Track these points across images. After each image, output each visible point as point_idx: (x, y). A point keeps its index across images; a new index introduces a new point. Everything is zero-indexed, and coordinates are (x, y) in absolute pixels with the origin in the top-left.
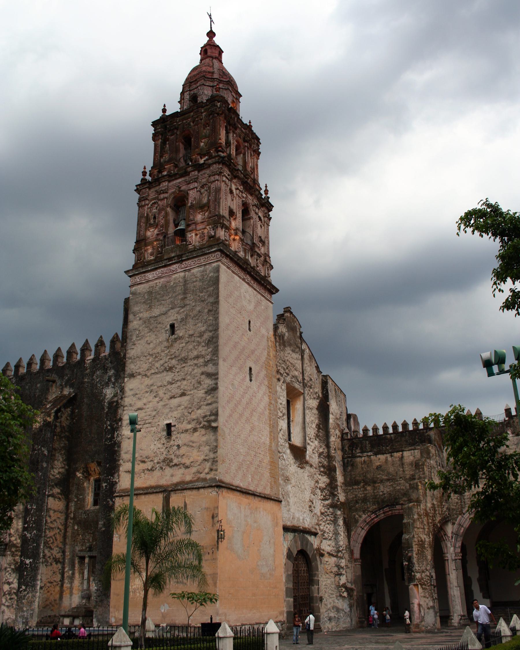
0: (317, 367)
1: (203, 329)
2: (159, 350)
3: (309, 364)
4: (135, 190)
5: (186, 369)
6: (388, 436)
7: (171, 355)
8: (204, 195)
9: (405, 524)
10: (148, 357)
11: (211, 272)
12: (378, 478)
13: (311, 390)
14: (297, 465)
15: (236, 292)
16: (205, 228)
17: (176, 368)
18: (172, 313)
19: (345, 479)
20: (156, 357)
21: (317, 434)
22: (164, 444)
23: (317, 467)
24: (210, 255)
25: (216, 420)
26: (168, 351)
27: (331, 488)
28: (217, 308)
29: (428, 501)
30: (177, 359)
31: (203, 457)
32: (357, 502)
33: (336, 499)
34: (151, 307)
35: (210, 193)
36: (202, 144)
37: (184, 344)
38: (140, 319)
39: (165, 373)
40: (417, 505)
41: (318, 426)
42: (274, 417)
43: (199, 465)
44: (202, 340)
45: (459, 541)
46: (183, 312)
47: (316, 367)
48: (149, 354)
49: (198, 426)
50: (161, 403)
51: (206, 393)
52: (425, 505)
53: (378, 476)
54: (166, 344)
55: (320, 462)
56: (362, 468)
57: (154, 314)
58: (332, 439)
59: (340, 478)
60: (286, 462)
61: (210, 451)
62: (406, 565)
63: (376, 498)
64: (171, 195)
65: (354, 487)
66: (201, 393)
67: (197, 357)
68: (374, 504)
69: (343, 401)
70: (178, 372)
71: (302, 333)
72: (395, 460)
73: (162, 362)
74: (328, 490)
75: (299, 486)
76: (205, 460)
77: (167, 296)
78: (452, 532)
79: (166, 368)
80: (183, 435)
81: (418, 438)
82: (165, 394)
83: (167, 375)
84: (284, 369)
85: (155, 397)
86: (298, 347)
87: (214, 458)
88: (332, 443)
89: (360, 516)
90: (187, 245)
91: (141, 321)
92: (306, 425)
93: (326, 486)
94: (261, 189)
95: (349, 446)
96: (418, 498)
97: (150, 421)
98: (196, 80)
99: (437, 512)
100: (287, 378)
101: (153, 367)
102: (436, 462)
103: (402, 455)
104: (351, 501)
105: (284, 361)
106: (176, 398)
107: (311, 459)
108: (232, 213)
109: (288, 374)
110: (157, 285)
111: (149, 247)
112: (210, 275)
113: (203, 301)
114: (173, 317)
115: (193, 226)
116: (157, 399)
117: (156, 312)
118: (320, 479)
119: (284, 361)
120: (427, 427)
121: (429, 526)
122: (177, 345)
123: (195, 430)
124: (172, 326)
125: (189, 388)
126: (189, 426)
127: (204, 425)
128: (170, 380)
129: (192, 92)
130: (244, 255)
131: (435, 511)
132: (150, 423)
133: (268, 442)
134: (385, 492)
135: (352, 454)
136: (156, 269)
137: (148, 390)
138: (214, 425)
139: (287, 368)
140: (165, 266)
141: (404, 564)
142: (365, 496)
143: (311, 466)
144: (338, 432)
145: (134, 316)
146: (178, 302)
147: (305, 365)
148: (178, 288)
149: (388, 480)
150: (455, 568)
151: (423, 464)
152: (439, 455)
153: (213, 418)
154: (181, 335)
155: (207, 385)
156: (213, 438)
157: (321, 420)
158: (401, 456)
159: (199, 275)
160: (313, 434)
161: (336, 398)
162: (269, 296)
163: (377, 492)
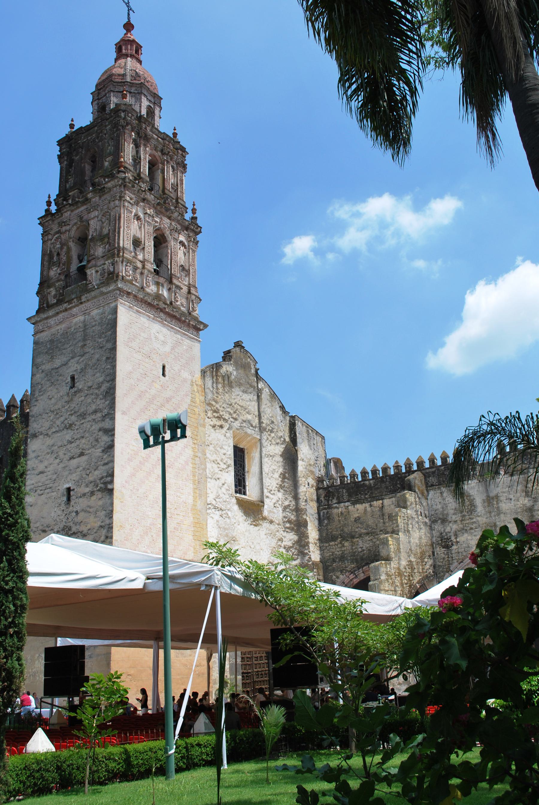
0: (282, 408)
1: (101, 379)
2: (59, 405)
3: (269, 404)
4: (39, 224)
5: (85, 425)
6: (367, 482)
7: (71, 411)
8: (105, 224)
9: (371, 586)
10: (49, 414)
11: (109, 314)
12: (357, 532)
13: (273, 435)
14: (249, 522)
15: (142, 334)
16: (105, 264)
17: (75, 425)
18: (72, 363)
19: (321, 535)
20: (57, 414)
21: (281, 485)
22: (63, 511)
23: (281, 523)
24: (109, 295)
25: (112, 482)
26: (68, 406)
27: (301, 546)
28: (115, 355)
29: (402, 558)
30: (76, 415)
31: (99, 523)
32: (334, 561)
33: (307, 558)
34: (52, 358)
35: (110, 221)
36: (106, 164)
37: (83, 398)
38: (43, 372)
39: (65, 432)
40: (386, 564)
41: (283, 476)
42: (201, 472)
43: (95, 533)
44: (99, 392)
46: (83, 361)
47: (280, 407)
48: (51, 411)
49: (95, 489)
50: (62, 465)
51: (103, 451)
52: (399, 563)
53: (357, 530)
54: (66, 398)
55: (284, 517)
56: (339, 521)
57: (55, 366)
58: (302, 489)
59: (313, 533)
60: (232, 520)
61: (106, 516)
63: (354, 556)
64: (73, 226)
65: (331, 544)
66: (98, 452)
67: (95, 412)
68: (352, 562)
69: (319, 444)
70: (77, 429)
71: (258, 369)
72: (374, 510)
73: (62, 419)
74: (296, 549)
75: (252, 546)
76: (101, 527)
77: (68, 344)
79: (66, 426)
80: (81, 500)
81: (400, 484)
82: (65, 454)
83: (68, 433)
84: (230, 414)
85: (56, 458)
86: (251, 386)
87: (110, 524)
88: (302, 494)
89: (338, 577)
90: (87, 284)
91: (44, 374)
92: (264, 475)
93: (293, 544)
94: (187, 208)
95: (326, 496)
96: (388, 555)
97: (51, 485)
98: (104, 86)
99: (416, 571)
100: (235, 424)
101: (54, 425)
102: (416, 511)
103: (382, 504)
104: (328, 560)
105: (231, 405)
106: (75, 458)
107: (271, 514)
108: (137, 243)
109: (236, 419)
110: (58, 333)
111: (52, 289)
112: (109, 317)
113: (101, 348)
114: (74, 367)
115: (93, 262)
116: (58, 461)
117: (58, 362)
118: (285, 537)
119: (231, 405)
120: (410, 471)
121: (403, 587)
122: (79, 399)
123: (92, 493)
124: (73, 378)
125: (87, 447)
126: (87, 490)
127: (101, 488)
128: (70, 439)
129: (101, 101)
130: (156, 289)
131: (413, 569)
132: (50, 488)
133: (190, 500)
134: (364, 548)
135: (328, 505)
136: (58, 313)
137: (49, 451)
138: (110, 487)
139: (235, 412)
140: (66, 310)
142: (343, 553)
143: (271, 522)
144: (312, 481)
145: (37, 368)
146: (78, 350)
147: (263, 406)
148: (79, 334)
149: (367, 534)
151: (397, 515)
152: (421, 502)
153: (109, 479)
154: (80, 387)
155: (104, 443)
156: (109, 501)
157: (287, 468)
158: (381, 505)
159: (97, 318)
160: (275, 485)
161: (309, 441)
162: (195, 333)
163: (356, 548)
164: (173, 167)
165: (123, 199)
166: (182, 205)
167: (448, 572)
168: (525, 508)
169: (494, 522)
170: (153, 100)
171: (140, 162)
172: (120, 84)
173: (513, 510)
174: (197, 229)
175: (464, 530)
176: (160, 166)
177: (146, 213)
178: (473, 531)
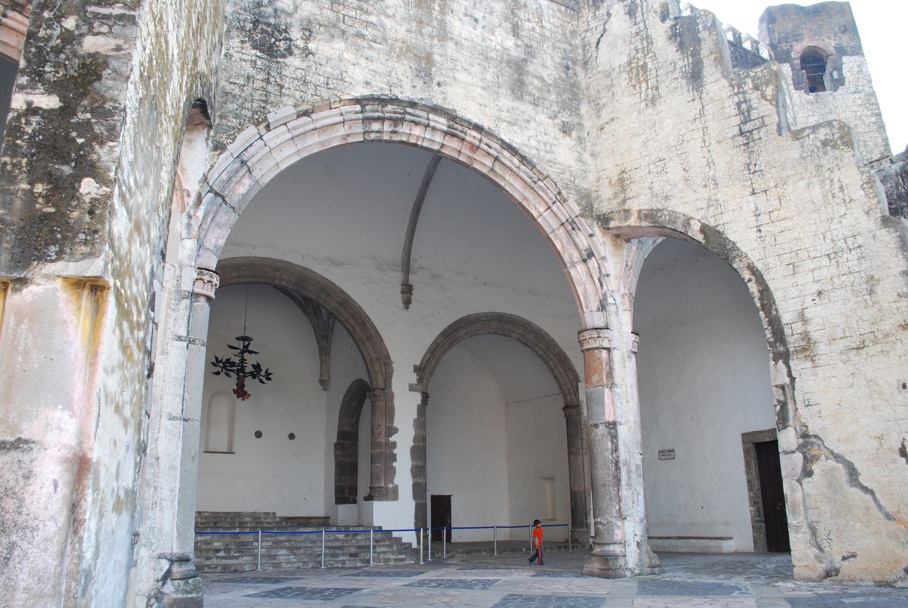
45: (219, 226)
62: (31, 110)
78: (205, 179)
141: (18, 101)
150: (183, 333)
167: (257, 124)
168: (506, 58)
169: (428, 49)
173: (479, 48)
175: (335, 29)
178: (365, 44)
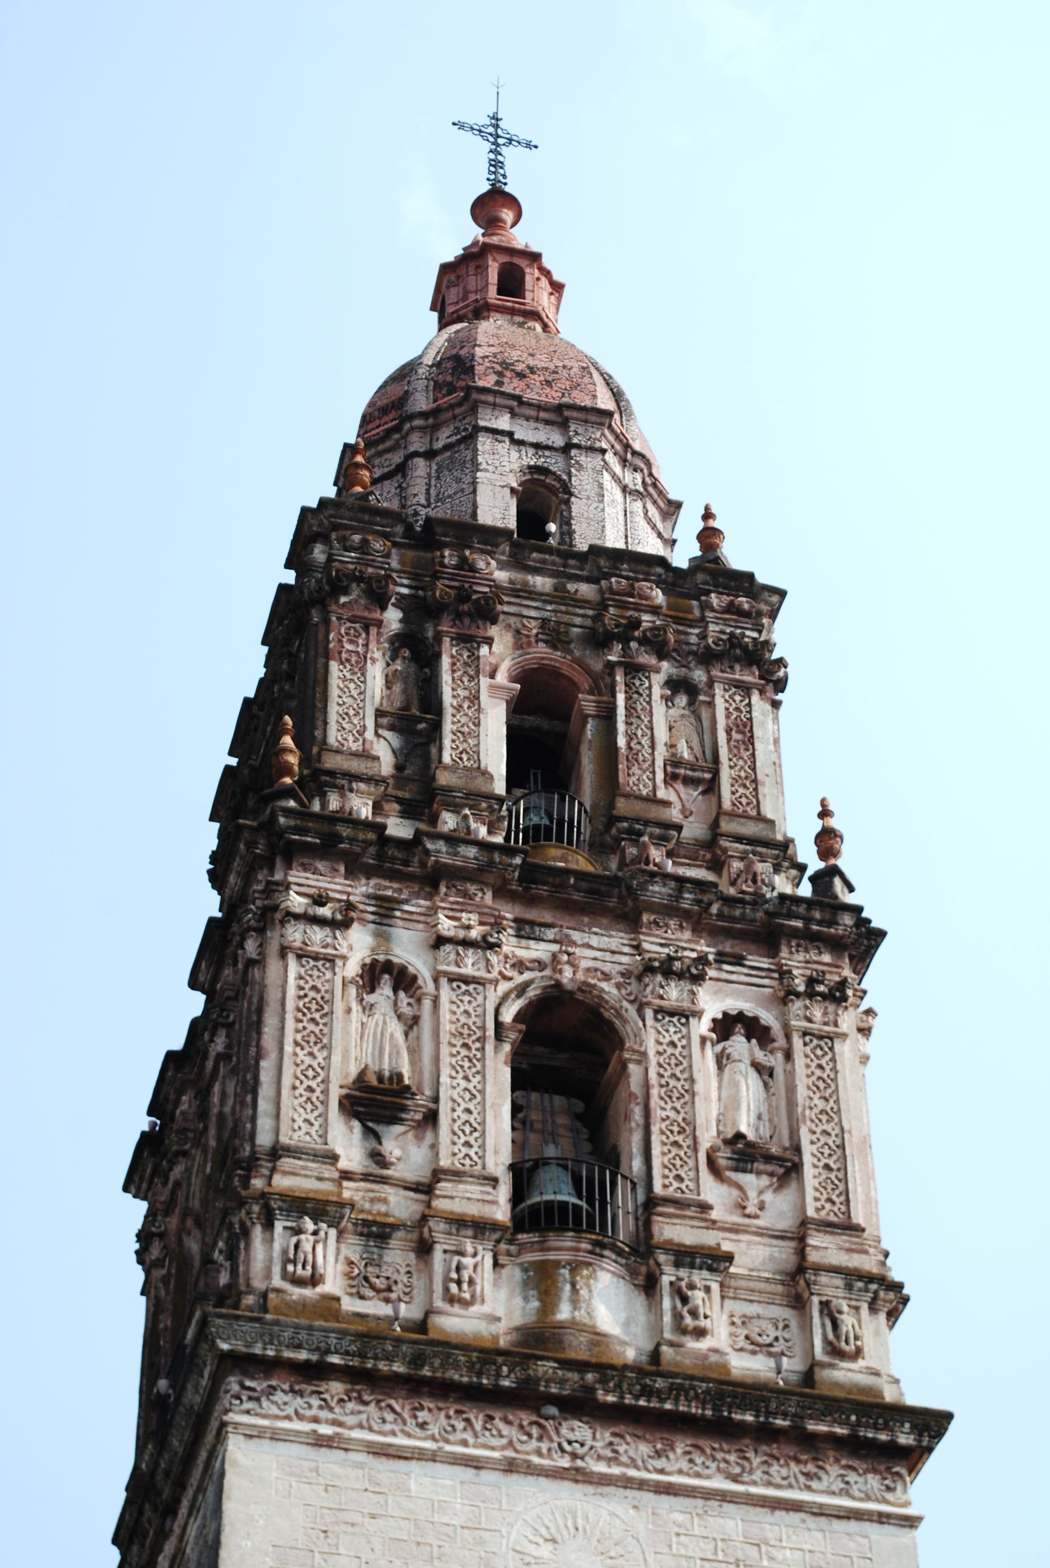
164: (676, 686)
165: (278, 916)
166: (739, 839)
170: (558, 441)
171: (436, 727)
172: (388, 444)
174: (833, 923)
176: (587, 703)
177: (440, 941)
